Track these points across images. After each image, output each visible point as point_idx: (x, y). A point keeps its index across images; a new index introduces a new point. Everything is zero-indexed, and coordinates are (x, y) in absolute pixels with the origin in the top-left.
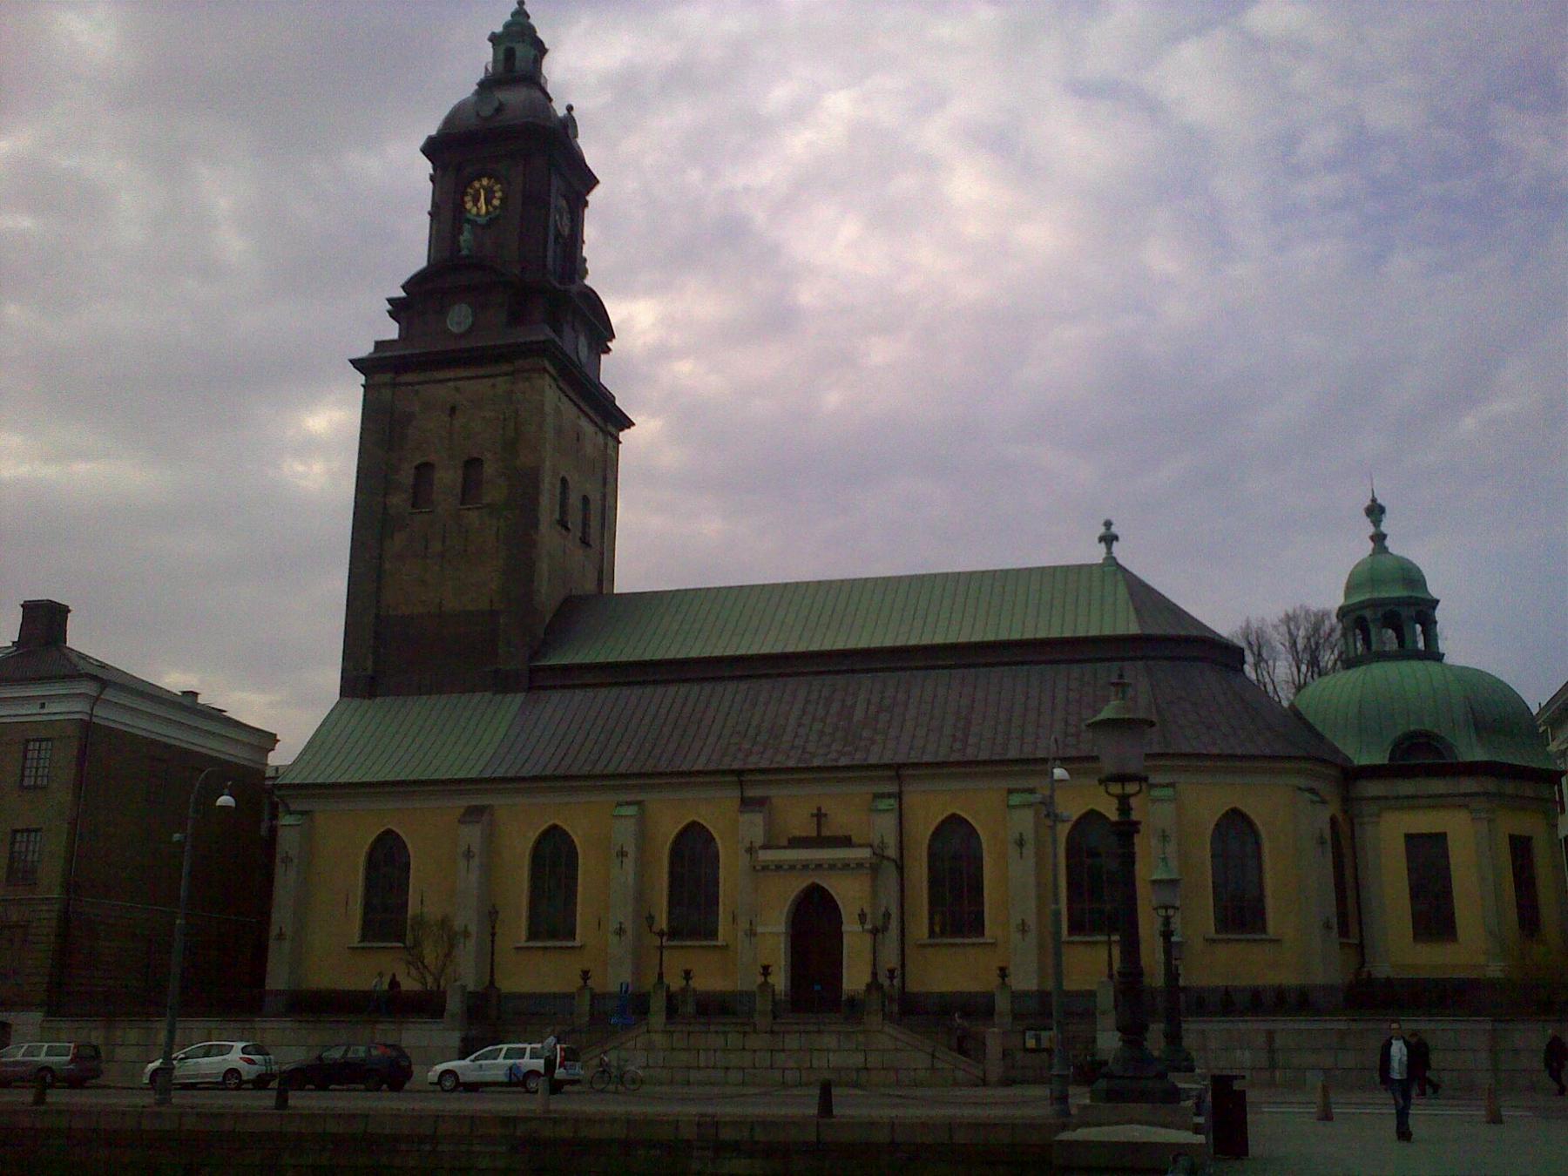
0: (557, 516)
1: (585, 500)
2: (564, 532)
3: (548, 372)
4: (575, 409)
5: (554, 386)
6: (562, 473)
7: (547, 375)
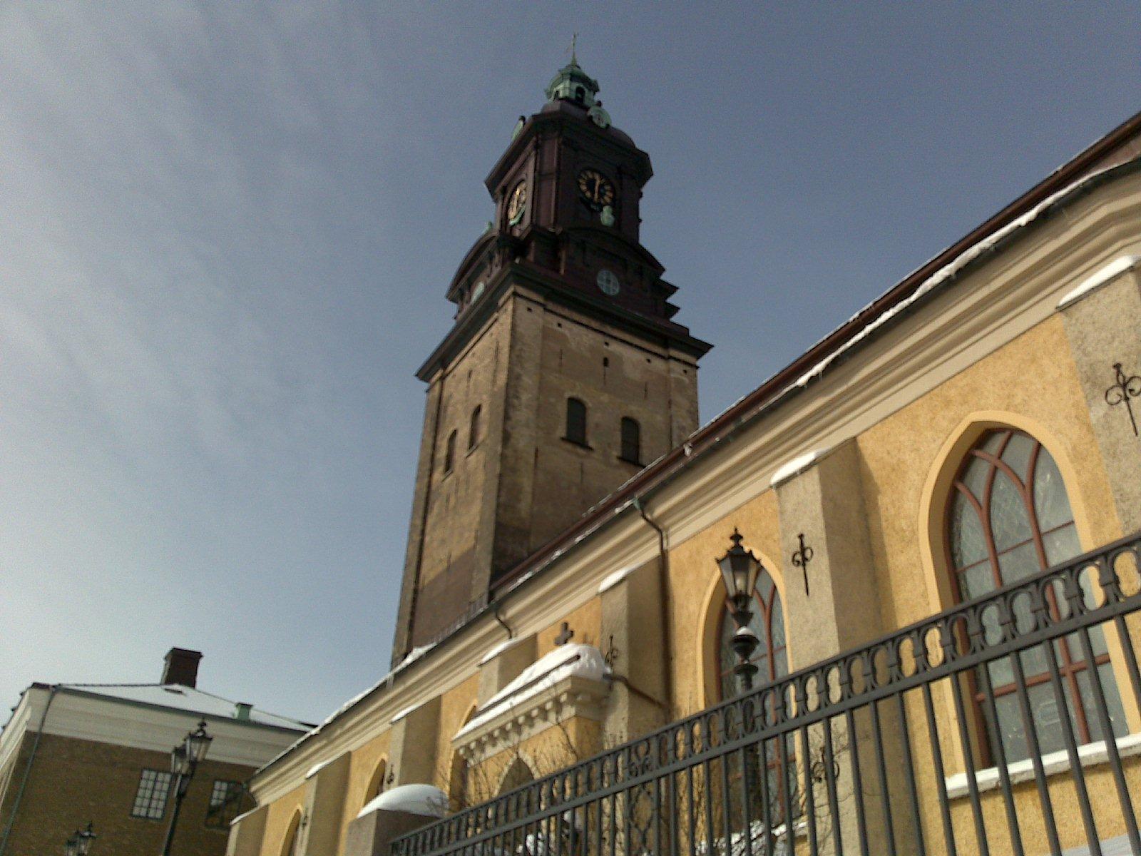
0: (561, 431)
1: (630, 426)
2: (581, 451)
3: (521, 296)
4: (600, 338)
5: (539, 310)
6: (568, 395)
7: (518, 299)
